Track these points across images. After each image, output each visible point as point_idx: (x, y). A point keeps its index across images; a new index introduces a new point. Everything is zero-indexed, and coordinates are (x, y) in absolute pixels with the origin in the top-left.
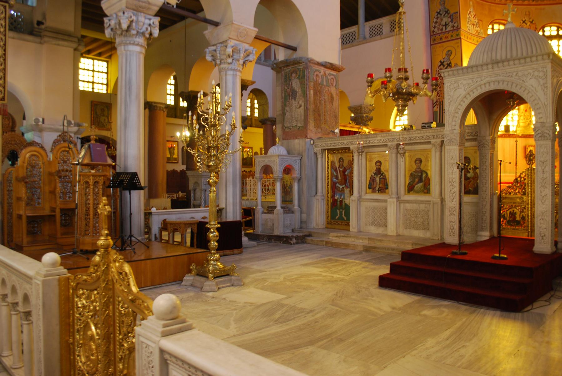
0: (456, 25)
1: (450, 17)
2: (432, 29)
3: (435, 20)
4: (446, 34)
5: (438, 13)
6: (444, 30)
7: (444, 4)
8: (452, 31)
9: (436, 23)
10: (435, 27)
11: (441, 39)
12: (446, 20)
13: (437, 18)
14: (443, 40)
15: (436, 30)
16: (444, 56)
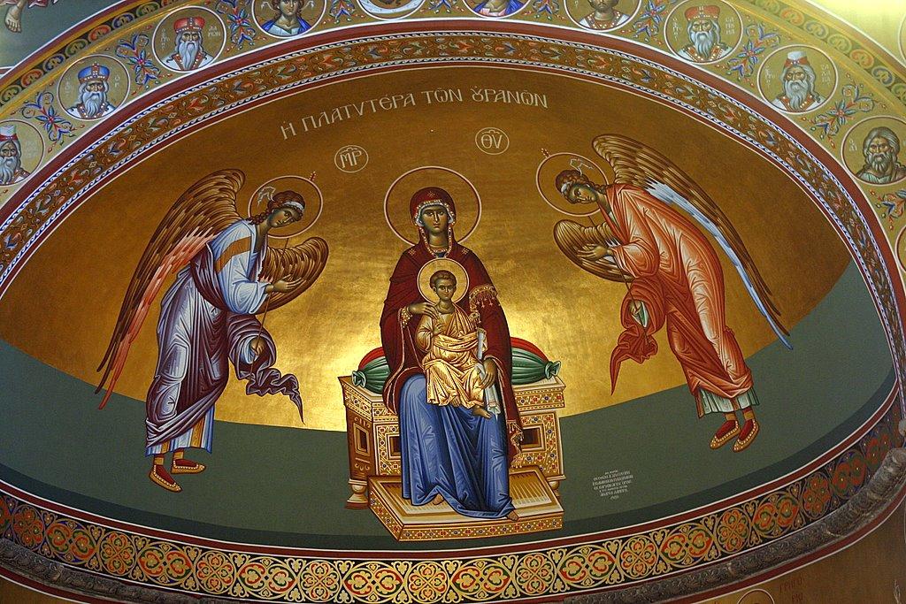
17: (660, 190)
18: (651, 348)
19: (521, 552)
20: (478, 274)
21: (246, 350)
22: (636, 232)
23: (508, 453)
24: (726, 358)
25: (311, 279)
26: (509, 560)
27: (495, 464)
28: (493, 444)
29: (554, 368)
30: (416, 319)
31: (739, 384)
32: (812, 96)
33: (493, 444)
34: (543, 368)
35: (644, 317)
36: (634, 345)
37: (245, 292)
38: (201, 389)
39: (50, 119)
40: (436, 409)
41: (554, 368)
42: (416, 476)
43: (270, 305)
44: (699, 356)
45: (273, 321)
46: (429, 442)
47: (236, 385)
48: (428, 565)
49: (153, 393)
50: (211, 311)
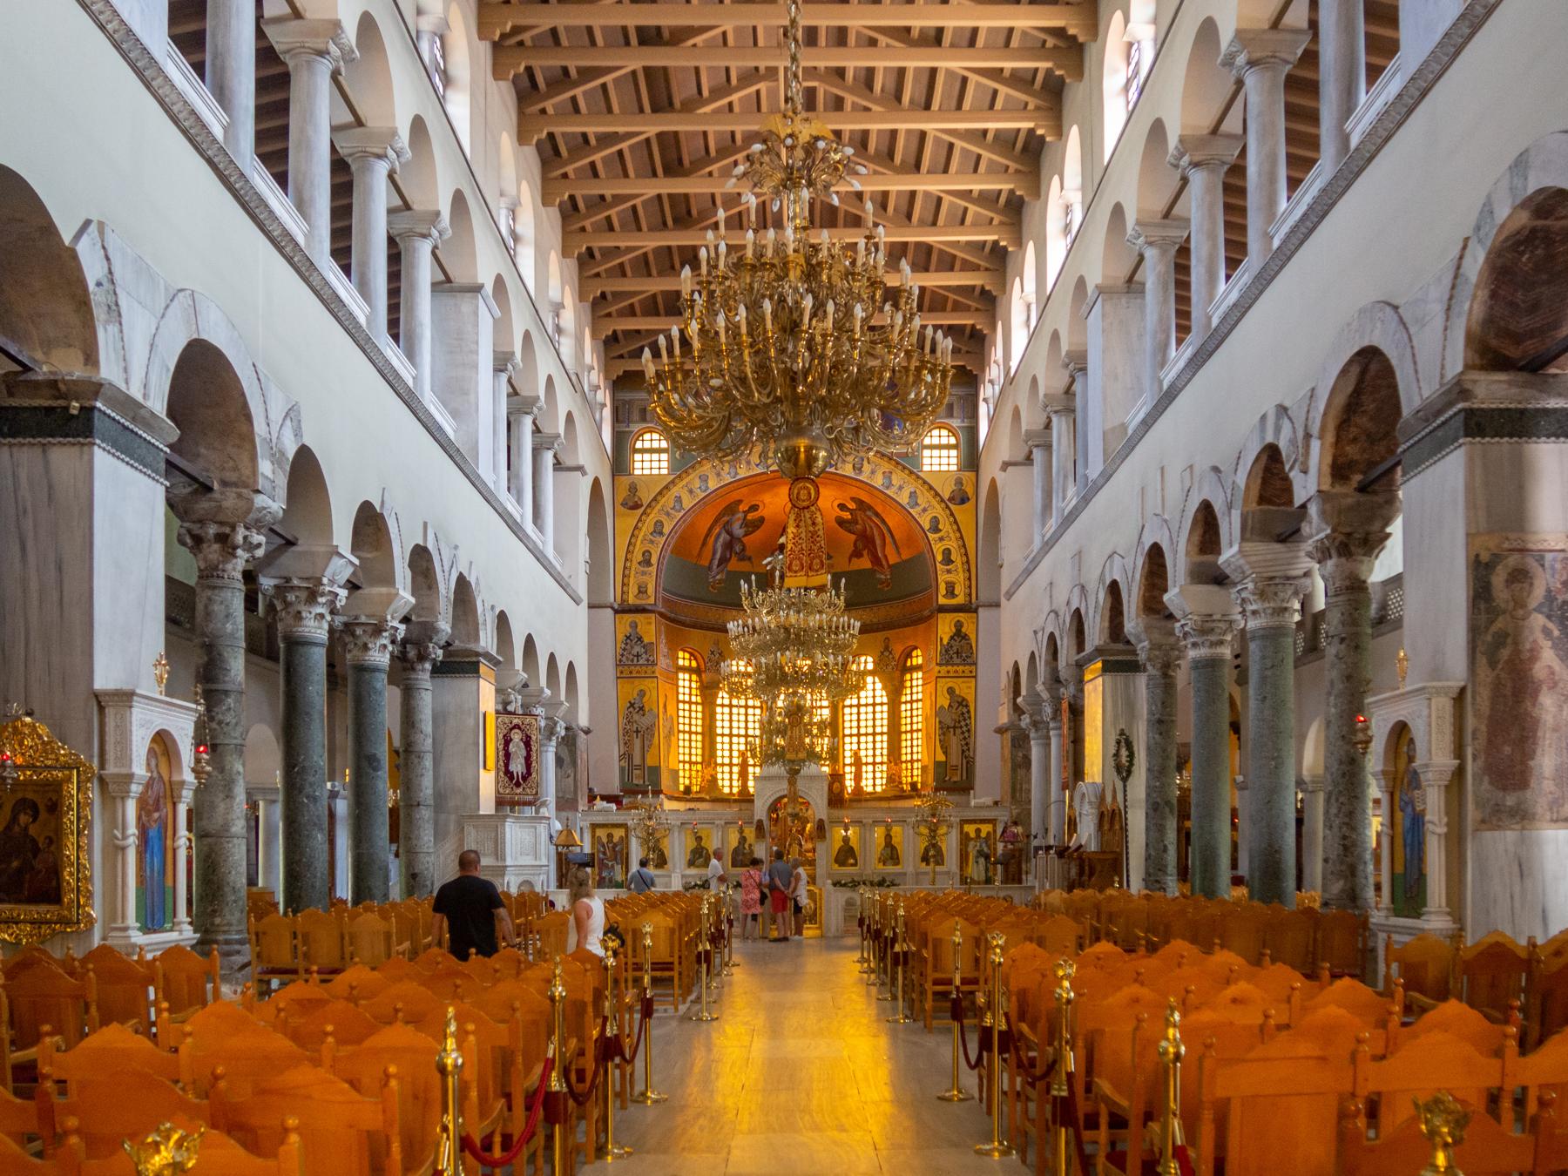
4: (638, 668)
5: (628, 638)
9: (624, 650)
15: (624, 659)
17: (869, 513)
21: (738, 548)
24: (884, 563)
32: (917, 504)
35: (860, 545)
37: (738, 530)
39: (691, 491)
43: (746, 535)
44: (876, 560)
45: (745, 540)
47: (734, 559)
50: (728, 537)
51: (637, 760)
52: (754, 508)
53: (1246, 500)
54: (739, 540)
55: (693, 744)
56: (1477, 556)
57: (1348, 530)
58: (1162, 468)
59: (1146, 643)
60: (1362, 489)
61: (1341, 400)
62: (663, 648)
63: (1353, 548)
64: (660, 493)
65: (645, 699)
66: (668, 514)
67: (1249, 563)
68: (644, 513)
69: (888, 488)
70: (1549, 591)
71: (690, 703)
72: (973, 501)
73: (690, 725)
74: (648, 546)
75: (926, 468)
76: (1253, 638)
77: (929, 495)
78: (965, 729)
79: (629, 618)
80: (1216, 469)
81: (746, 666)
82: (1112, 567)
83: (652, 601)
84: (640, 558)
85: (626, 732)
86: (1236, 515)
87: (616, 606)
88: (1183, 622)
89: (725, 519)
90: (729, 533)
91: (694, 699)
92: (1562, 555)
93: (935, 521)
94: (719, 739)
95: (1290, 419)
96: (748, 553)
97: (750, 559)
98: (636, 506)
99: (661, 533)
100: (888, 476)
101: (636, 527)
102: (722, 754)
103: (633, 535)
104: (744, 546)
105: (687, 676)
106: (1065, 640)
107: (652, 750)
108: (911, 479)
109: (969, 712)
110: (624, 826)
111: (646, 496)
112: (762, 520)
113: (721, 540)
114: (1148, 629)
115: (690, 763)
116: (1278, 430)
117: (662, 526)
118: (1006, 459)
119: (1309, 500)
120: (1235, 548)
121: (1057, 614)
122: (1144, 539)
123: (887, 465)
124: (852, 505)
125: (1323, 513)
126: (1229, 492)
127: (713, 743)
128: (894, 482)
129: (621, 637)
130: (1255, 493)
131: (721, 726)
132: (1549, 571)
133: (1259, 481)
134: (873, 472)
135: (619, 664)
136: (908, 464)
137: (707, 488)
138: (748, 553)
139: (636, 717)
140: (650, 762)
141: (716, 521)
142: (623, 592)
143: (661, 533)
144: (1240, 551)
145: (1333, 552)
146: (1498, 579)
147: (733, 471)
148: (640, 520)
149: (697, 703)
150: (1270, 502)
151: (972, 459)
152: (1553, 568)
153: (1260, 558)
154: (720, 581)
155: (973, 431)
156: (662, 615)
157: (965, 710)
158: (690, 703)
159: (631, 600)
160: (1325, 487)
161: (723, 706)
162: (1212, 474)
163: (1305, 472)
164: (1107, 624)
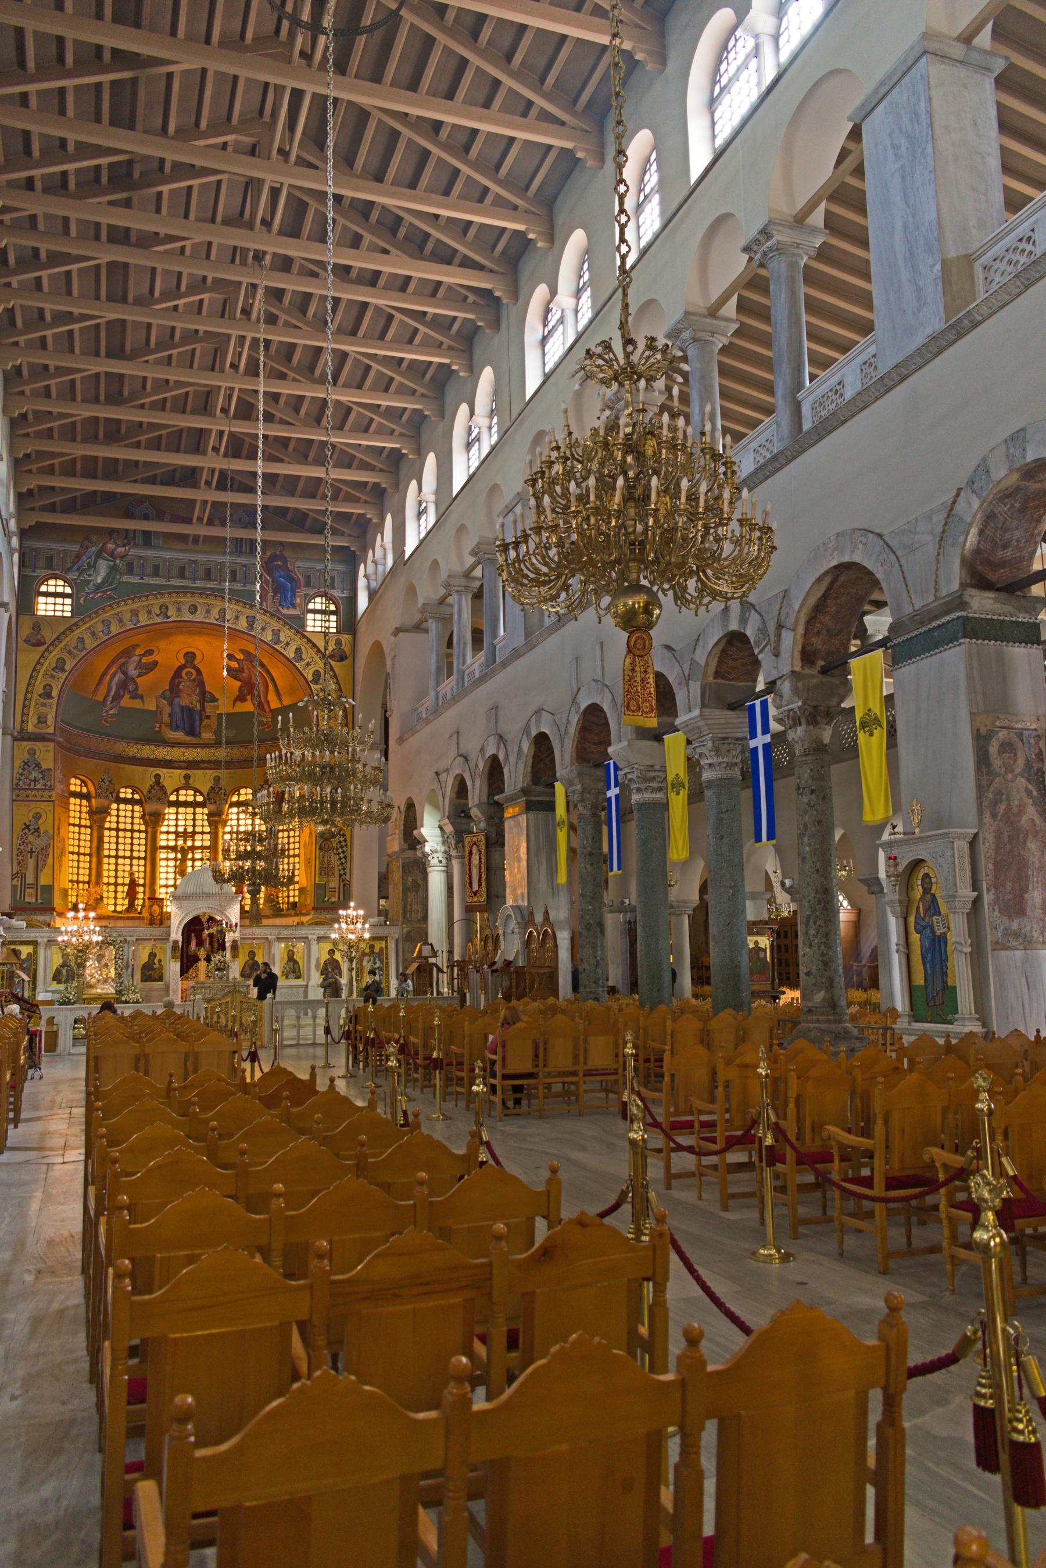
0: (49, 784)
1: (42, 772)
2: (15, 781)
3: (20, 771)
4: (34, 792)
5: (26, 764)
6: (32, 786)
7: (35, 753)
8: (44, 790)
9: (22, 774)
10: (19, 780)
11: (27, 796)
12: (35, 774)
13: (24, 769)
14: (31, 798)
15: (21, 783)
16: (31, 818)
18: (246, 700)
19: (203, 748)
20: (199, 672)
21: (131, 687)
22: (246, 671)
23: (201, 721)
24: (266, 707)
25: (152, 670)
26: (199, 750)
27: (197, 723)
28: (197, 717)
29: (217, 700)
30: (180, 682)
31: (269, 715)
33: (197, 717)
34: (214, 700)
36: (241, 698)
37: (132, 672)
38: (117, 697)
39: (93, 634)
40: (182, 708)
41: (217, 700)
42: (174, 724)
43: (140, 676)
45: (138, 680)
46: (179, 715)
47: (127, 696)
48: (176, 749)
49: (105, 699)
50: (123, 677)
51: (30, 879)
52: (150, 652)
53: (705, 674)
54: (133, 680)
55: (82, 865)
56: (978, 730)
57: (814, 704)
58: (602, 643)
59: (579, 787)
60: (824, 671)
61: (812, 601)
62: (59, 775)
63: (819, 718)
64: (63, 633)
65: (40, 822)
66: (70, 652)
67: (707, 725)
68: (47, 650)
69: (276, 643)
70: (1027, 760)
71: (80, 826)
72: (350, 659)
73: (79, 846)
74: (50, 681)
75: (309, 629)
76: (709, 787)
77: (312, 652)
78: (342, 855)
79: (27, 745)
80: (668, 648)
81: (133, 793)
82: (538, 721)
83: (51, 730)
84: (41, 691)
85: (20, 852)
86: (695, 687)
87: (16, 734)
88: (627, 770)
89: (122, 660)
90: (125, 673)
91: (83, 822)
92: (1034, 733)
93: (317, 675)
94: (106, 860)
95: (756, 611)
96: (140, 692)
97: (141, 697)
98: (39, 644)
99: (63, 670)
100: (276, 633)
101: (38, 663)
102: (108, 875)
103: (34, 670)
104: (136, 684)
105: (78, 801)
106: (478, 783)
107: (45, 870)
108: (297, 637)
109: (345, 840)
110: (34, 943)
111: (49, 636)
112: (155, 664)
113: (116, 679)
114: (580, 775)
115: (78, 882)
116: (743, 620)
117: (64, 663)
118: (398, 626)
119: (780, 678)
120: (696, 712)
121: (466, 759)
122: (579, 699)
123: (275, 624)
124: (240, 656)
125: (795, 690)
126: (686, 668)
127: (100, 863)
128: (282, 639)
129: (18, 763)
130: (712, 669)
131: (108, 848)
132: (1026, 745)
133: (717, 659)
134: (263, 629)
135: (15, 788)
136: (298, 625)
137: (109, 632)
138: (140, 692)
139: (31, 838)
140: (44, 880)
141: (113, 662)
142: (22, 722)
143: (63, 670)
144: (701, 715)
145: (803, 720)
146: (993, 749)
147: (134, 619)
148: (42, 656)
149: (86, 827)
150: (723, 677)
151: (349, 623)
152: (1029, 742)
153: (717, 721)
154: (112, 716)
155: (353, 600)
156: (59, 744)
157: (342, 839)
158: (80, 826)
159: (30, 728)
160: (797, 669)
161: (110, 829)
162: (665, 651)
163: (777, 655)
164: (529, 769)
